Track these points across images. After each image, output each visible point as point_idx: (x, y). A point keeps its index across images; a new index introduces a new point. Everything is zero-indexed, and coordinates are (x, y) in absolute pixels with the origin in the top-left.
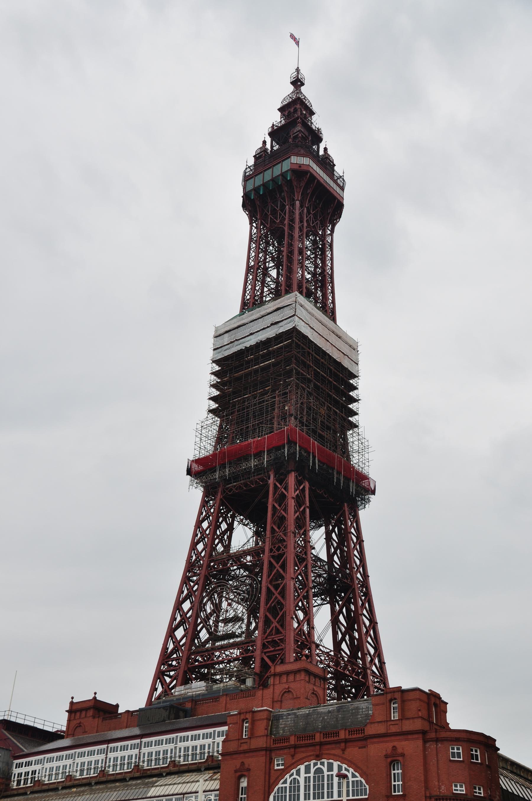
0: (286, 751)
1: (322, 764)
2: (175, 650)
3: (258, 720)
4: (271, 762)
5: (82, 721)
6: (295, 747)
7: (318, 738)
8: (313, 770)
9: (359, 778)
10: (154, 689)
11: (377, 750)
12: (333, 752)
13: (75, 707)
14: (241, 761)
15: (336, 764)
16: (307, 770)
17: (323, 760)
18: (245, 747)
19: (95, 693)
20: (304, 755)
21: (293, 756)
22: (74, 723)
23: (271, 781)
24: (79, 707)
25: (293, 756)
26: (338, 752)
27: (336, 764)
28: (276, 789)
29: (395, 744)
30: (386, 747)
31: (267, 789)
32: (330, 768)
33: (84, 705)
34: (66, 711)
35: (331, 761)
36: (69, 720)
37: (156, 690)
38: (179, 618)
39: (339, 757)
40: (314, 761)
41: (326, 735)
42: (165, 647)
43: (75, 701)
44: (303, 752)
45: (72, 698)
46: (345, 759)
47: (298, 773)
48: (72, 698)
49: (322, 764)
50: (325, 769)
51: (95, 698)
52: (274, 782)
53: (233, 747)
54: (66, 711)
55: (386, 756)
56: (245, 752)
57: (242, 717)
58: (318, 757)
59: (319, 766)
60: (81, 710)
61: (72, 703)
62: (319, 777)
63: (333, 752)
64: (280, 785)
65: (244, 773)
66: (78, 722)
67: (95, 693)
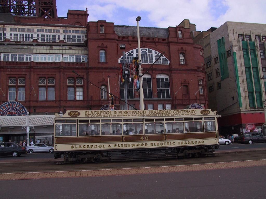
0: (126, 42)
1: (146, 50)
9: (165, 57)
11: (174, 48)
12: (152, 46)
15: (153, 51)
17: (146, 48)
25: (130, 45)
26: (155, 46)
27: (153, 51)
29: (183, 47)
30: (179, 47)
32: (150, 52)
35: (150, 49)
39: (155, 48)
46: (158, 49)
47: (132, 52)
49: (146, 50)
50: (148, 52)
55: (178, 50)
56: (103, 39)
59: (144, 50)
63: (152, 46)
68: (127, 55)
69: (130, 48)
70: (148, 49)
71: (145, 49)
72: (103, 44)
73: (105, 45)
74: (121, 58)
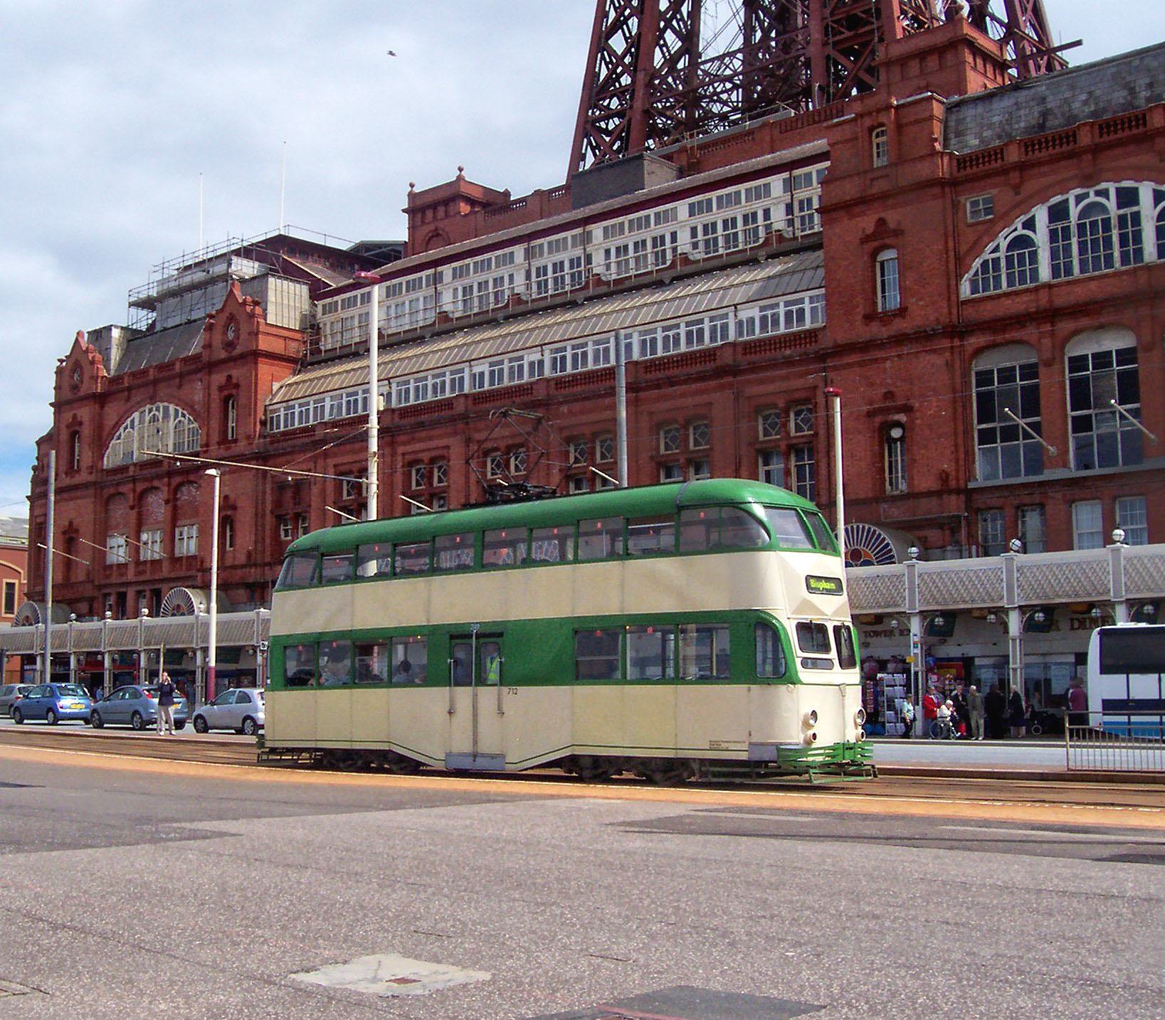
2: (613, 78)
3: (911, 123)
4: (956, 206)
5: (440, 225)
6: (1022, 167)
7: (1085, 139)
8: (1074, 211)
10: (577, 157)
12: (1133, 160)
13: (419, 202)
14: (876, 217)
16: (1059, 213)
17: (1103, 185)
18: (881, 186)
19: (461, 170)
20: (1045, 181)
21: (1017, 189)
22: (424, 231)
23: (964, 248)
24: (428, 199)
25: (1017, 189)
28: (977, 264)
31: (952, 267)
32: (1128, 198)
33: (441, 195)
34: (404, 211)
36: (412, 228)
37: (583, 157)
38: (612, 15)
40: (1078, 191)
41: (1105, 127)
42: (591, 74)
43: (416, 190)
44: (1045, 175)
45: (412, 186)
48: (412, 186)
49: (1104, 193)
50: (1111, 204)
51: (460, 178)
52: (971, 249)
53: (849, 190)
54: (404, 211)
57: (868, 122)
58: (1088, 180)
59: (1093, 198)
60: (434, 206)
61: (412, 196)
62: (1021, 256)
64: (987, 255)
65: (887, 241)
66: (432, 227)
67: (461, 170)
68: (1004, 245)
69: (1017, 206)
70: (1111, 187)
71: (1098, 193)
72: (881, 222)
73: (892, 225)
74: (972, 272)
